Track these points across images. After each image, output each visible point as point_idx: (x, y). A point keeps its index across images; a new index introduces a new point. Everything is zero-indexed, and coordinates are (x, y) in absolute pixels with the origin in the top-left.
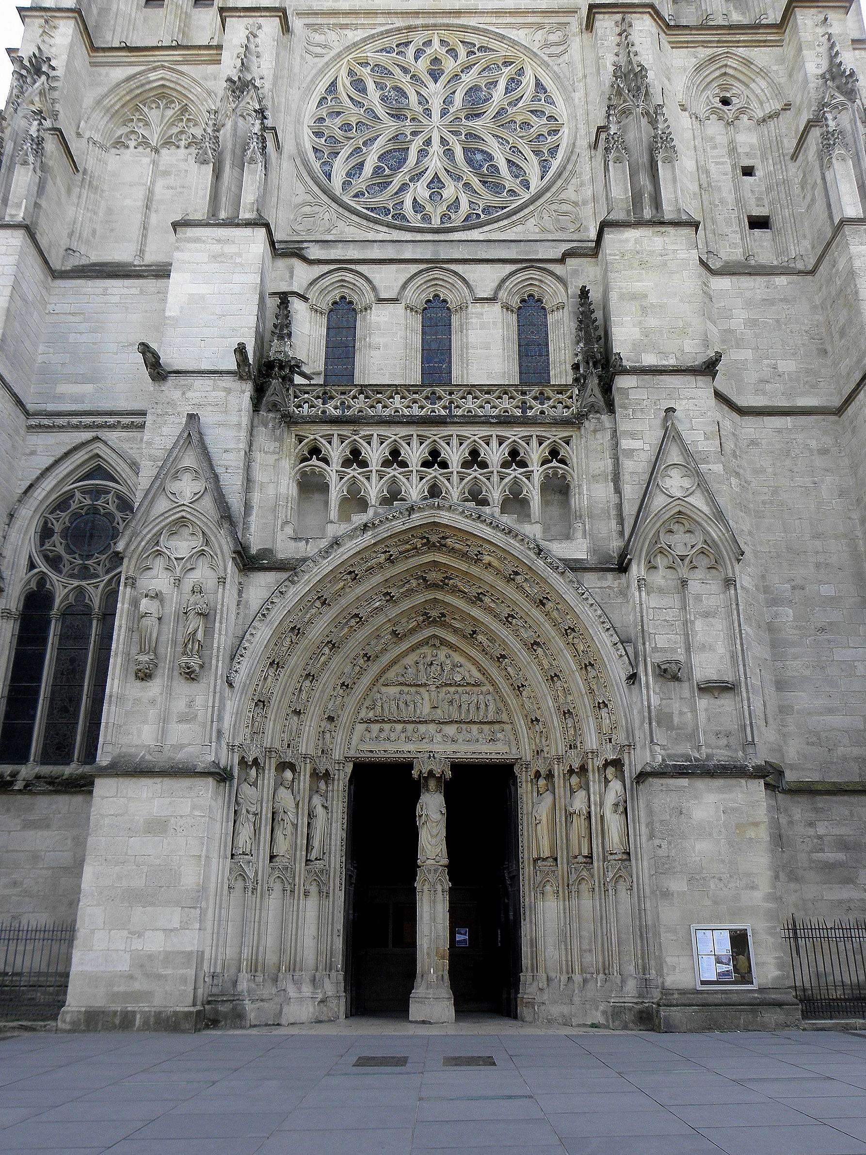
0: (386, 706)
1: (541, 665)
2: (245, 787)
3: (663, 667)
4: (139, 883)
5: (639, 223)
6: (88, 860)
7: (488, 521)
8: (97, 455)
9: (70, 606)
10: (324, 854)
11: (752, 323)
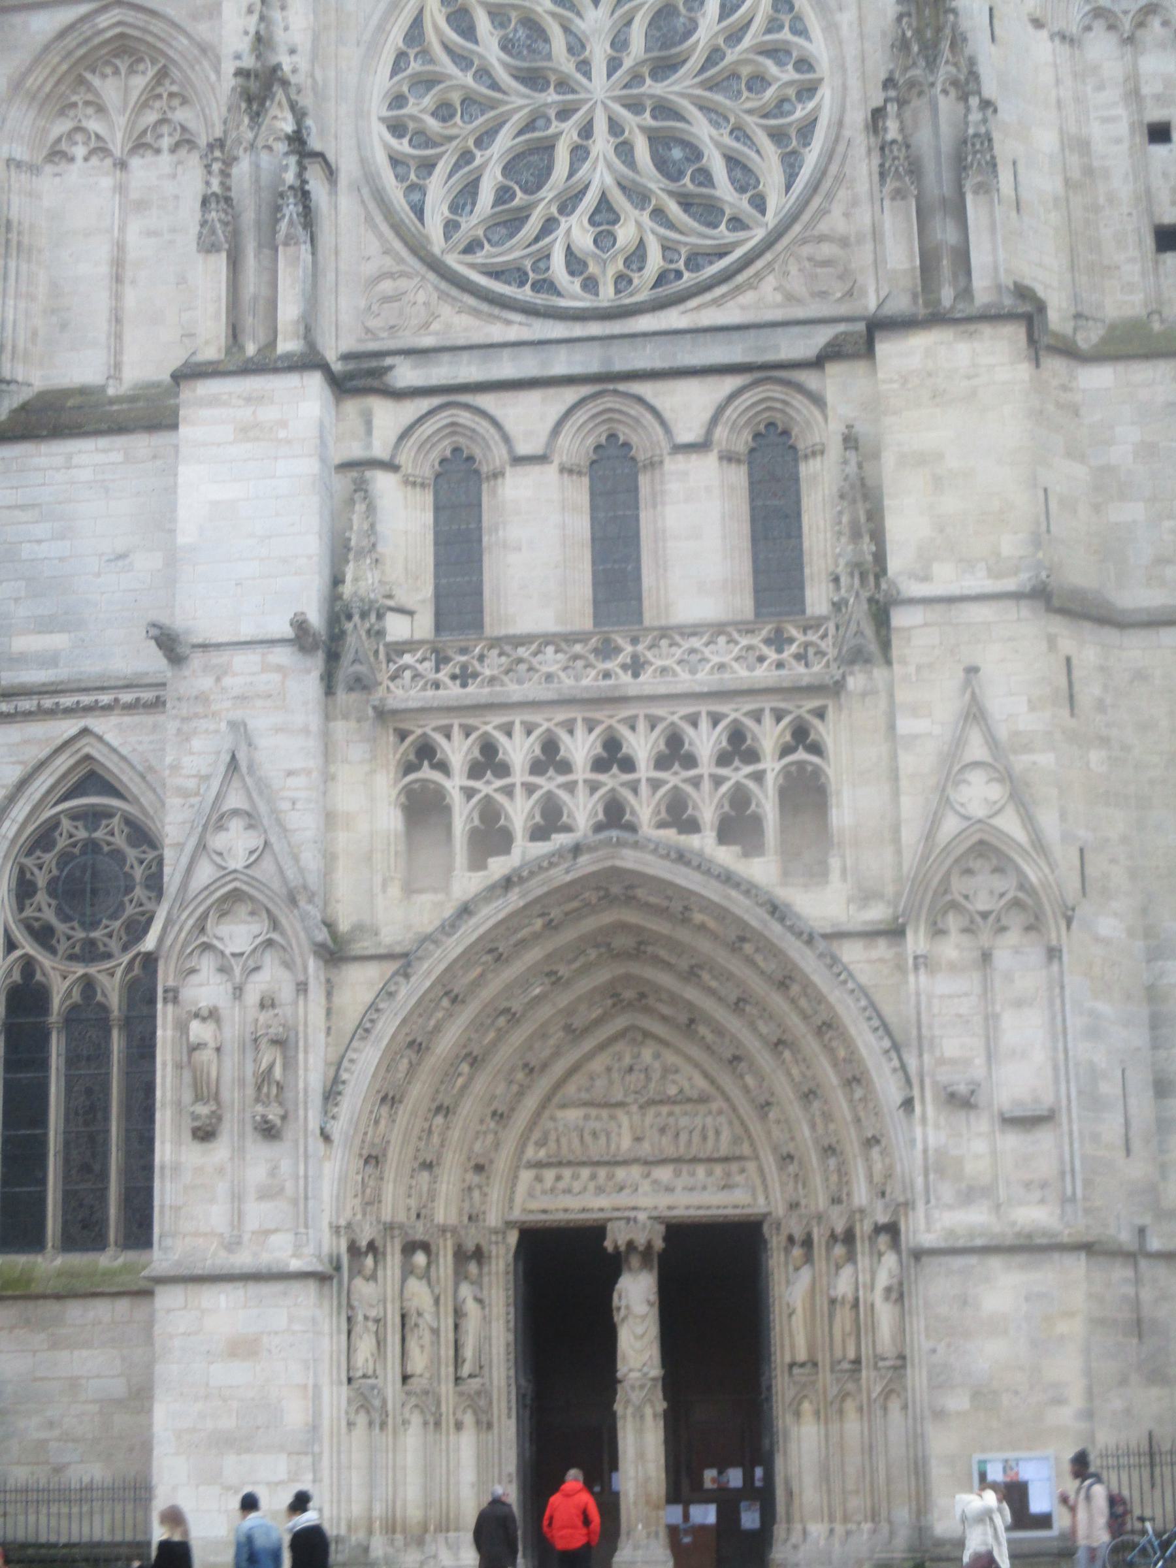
0: (564, 1141)
1: (789, 1074)
2: (359, 1282)
3: (950, 1089)
4: (228, 1423)
5: (936, 319)
6: (159, 1393)
7: (695, 863)
8: (88, 757)
9: (74, 1008)
10: (481, 1367)
11: (1147, 451)
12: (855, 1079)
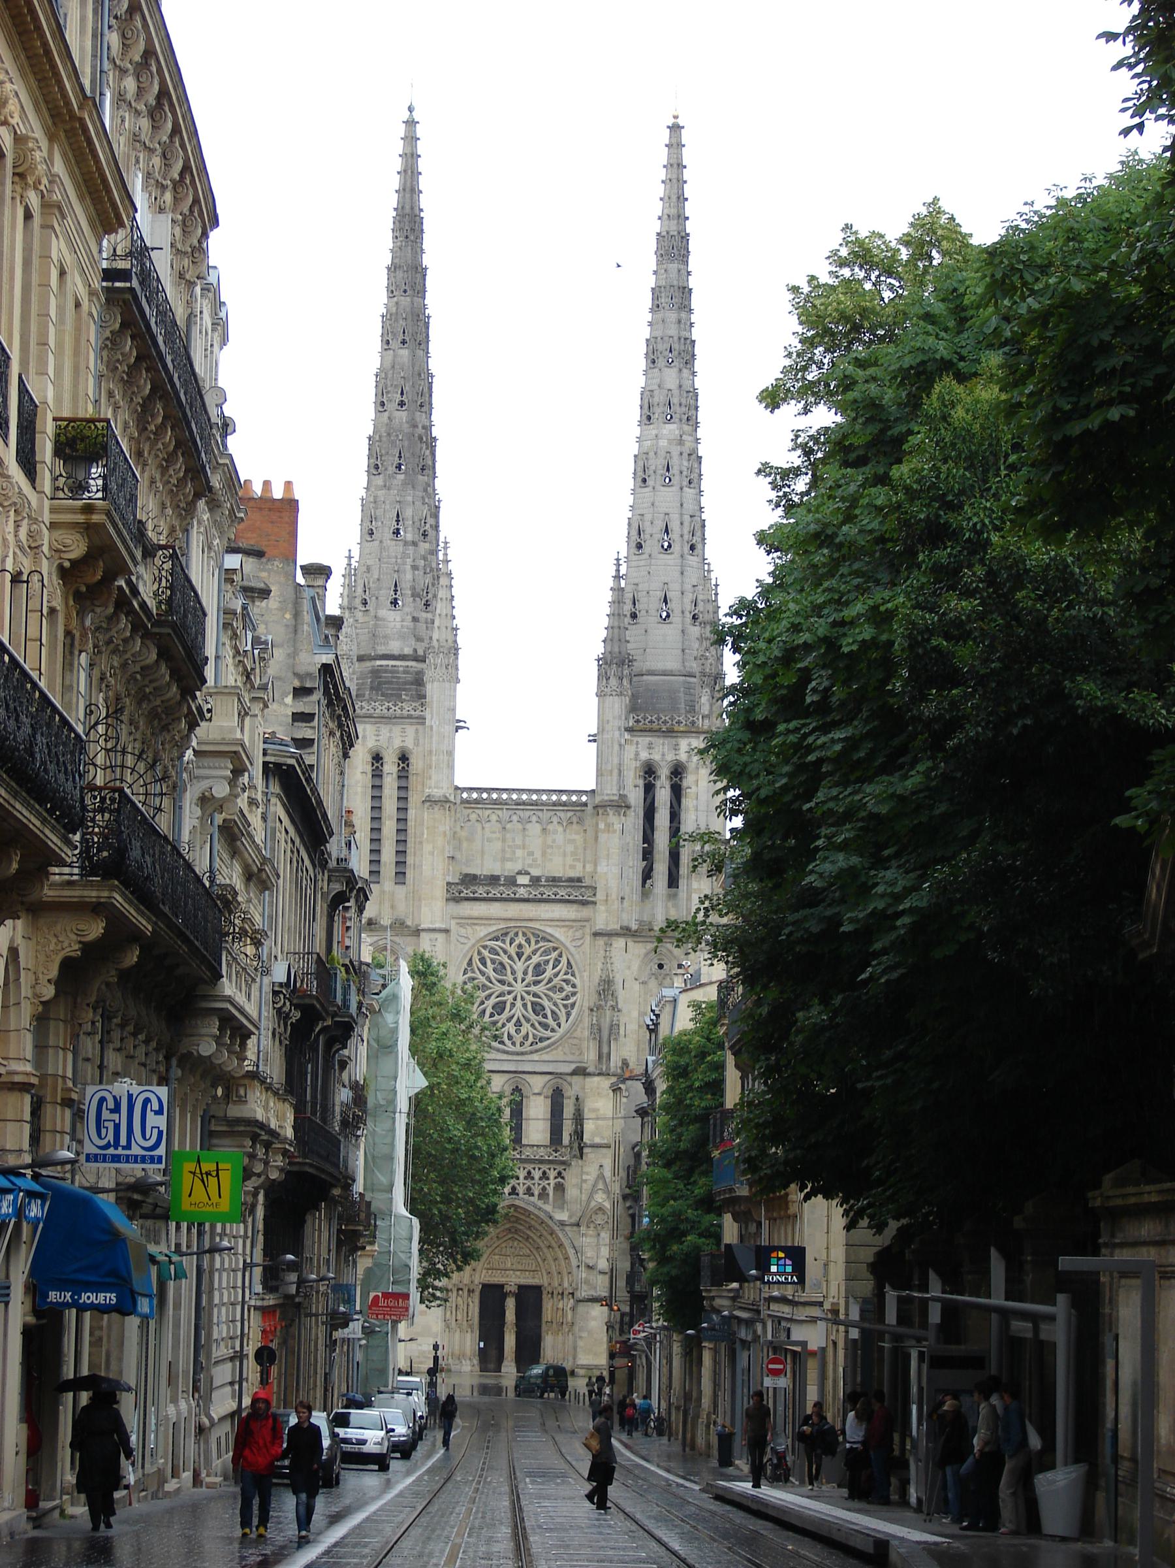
5: (599, 1074)
12: (567, 1258)
